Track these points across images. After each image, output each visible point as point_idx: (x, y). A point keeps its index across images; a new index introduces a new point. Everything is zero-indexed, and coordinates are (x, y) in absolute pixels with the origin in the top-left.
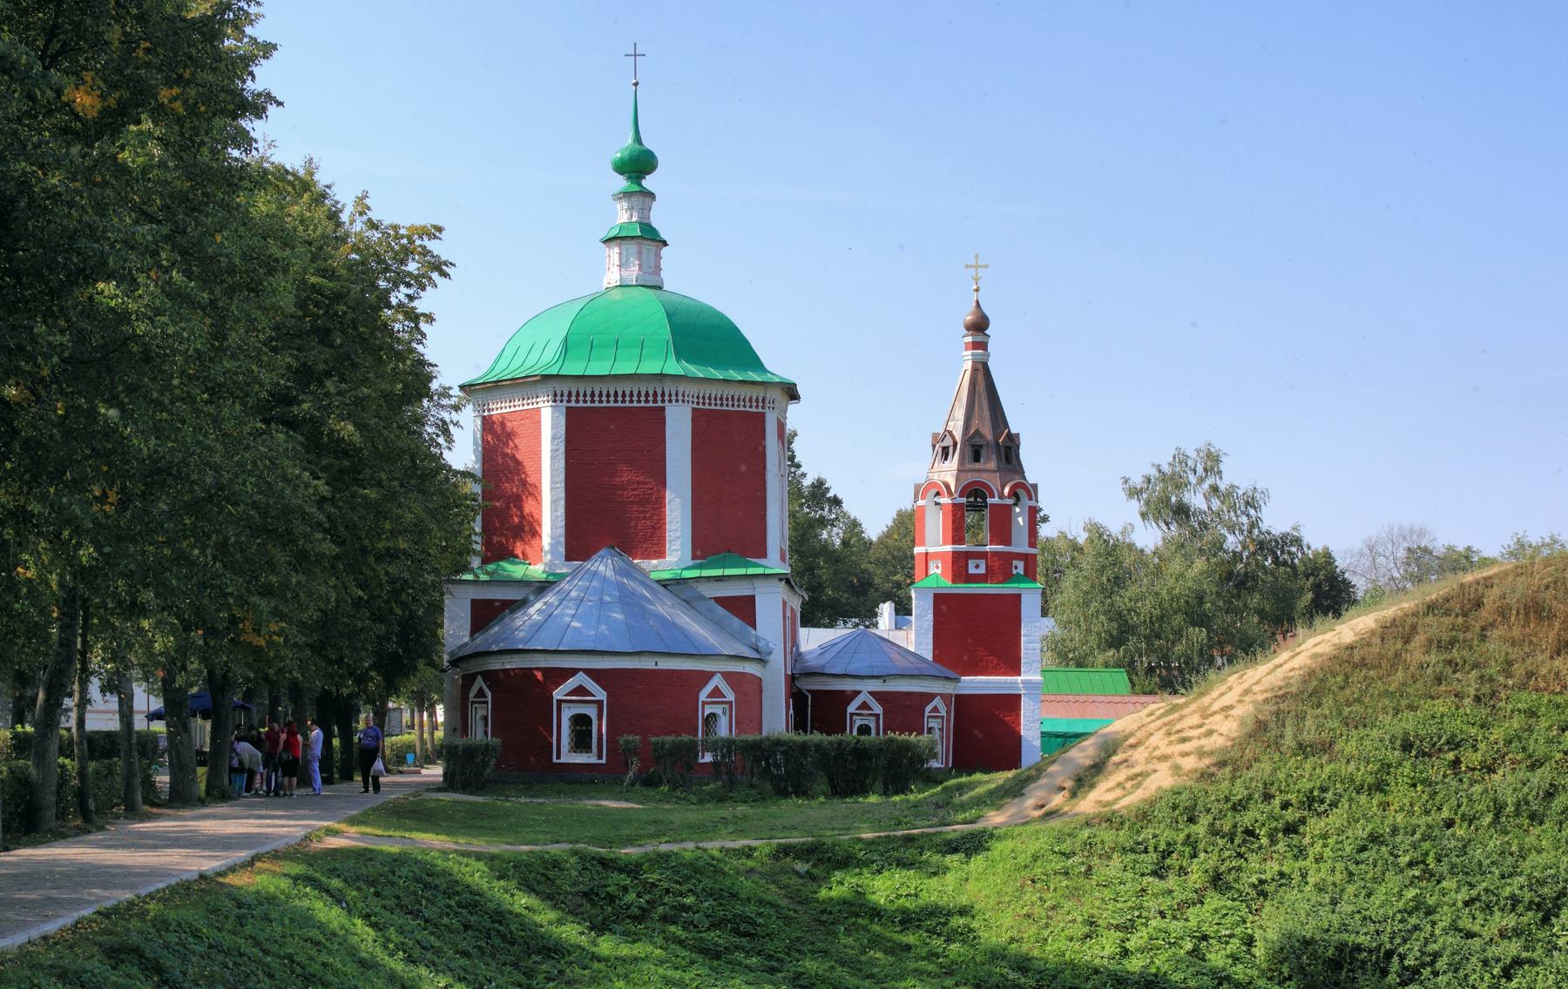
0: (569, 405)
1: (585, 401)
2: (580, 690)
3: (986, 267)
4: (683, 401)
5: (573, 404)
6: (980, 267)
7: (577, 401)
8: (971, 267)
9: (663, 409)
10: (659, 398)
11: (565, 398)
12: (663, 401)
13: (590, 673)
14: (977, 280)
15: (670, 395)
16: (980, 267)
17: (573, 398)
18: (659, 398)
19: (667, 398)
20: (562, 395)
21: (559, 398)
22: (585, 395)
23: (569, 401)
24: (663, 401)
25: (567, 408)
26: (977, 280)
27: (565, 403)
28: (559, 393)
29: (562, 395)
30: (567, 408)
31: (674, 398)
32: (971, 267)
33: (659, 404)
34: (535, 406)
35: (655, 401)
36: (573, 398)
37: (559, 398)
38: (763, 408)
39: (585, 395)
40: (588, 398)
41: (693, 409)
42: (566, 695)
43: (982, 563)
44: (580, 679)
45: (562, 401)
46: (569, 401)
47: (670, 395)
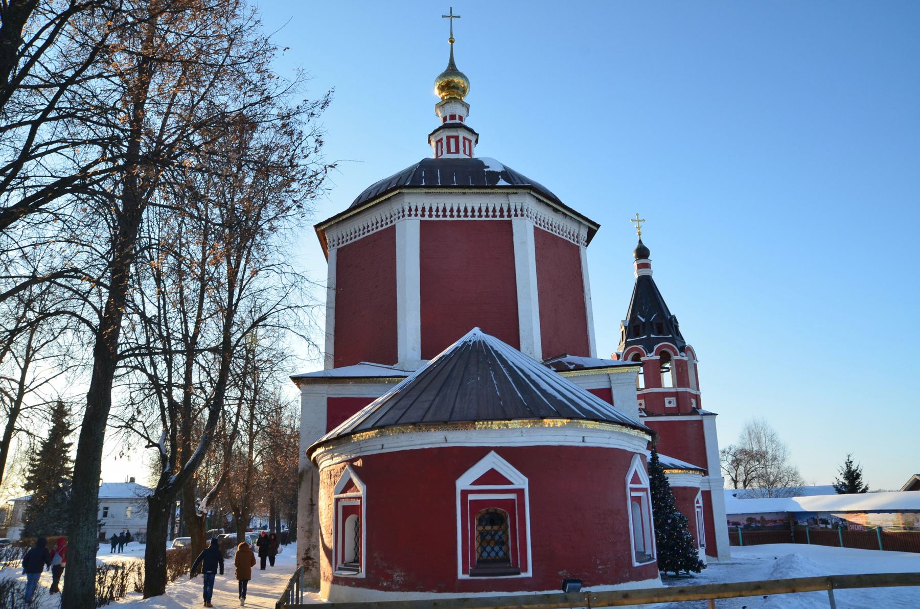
0: (423, 219)
1: (437, 216)
2: (492, 477)
3: (644, 220)
4: (527, 216)
5: (427, 218)
6: (640, 221)
7: (430, 216)
8: (636, 221)
9: (510, 223)
10: (506, 214)
11: (420, 212)
12: (509, 216)
13: (506, 453)
14: (639, 228)
15: (516, 210)
16: (640, 221)
17: (427, 213)
18: (506, 214)
19: (513, 213)
20: (416, 210)
21: (413, 213)
22: (437, 210)
23: (423, 215)
24: (509, 216)
25: (421, 221)
26: (639, 228)
27: (419, 216)
28: (413, 208)
29: (416, 210)
30: (421, 222)
31: (519, 212)
32: (636, 221)
33: (506, 218)
34: (389, 225)
35: (502, 216)
36: (427, 213)
37: (413, 213)
38: (578, 242)
39: (437, 210)
40: (441, 213)
41: (534, 226)
42: (474, 483)
43: (673, 399)
44: (492, 462)
45: (416, 215)
46: (423, 215)
47: (516, 210)
